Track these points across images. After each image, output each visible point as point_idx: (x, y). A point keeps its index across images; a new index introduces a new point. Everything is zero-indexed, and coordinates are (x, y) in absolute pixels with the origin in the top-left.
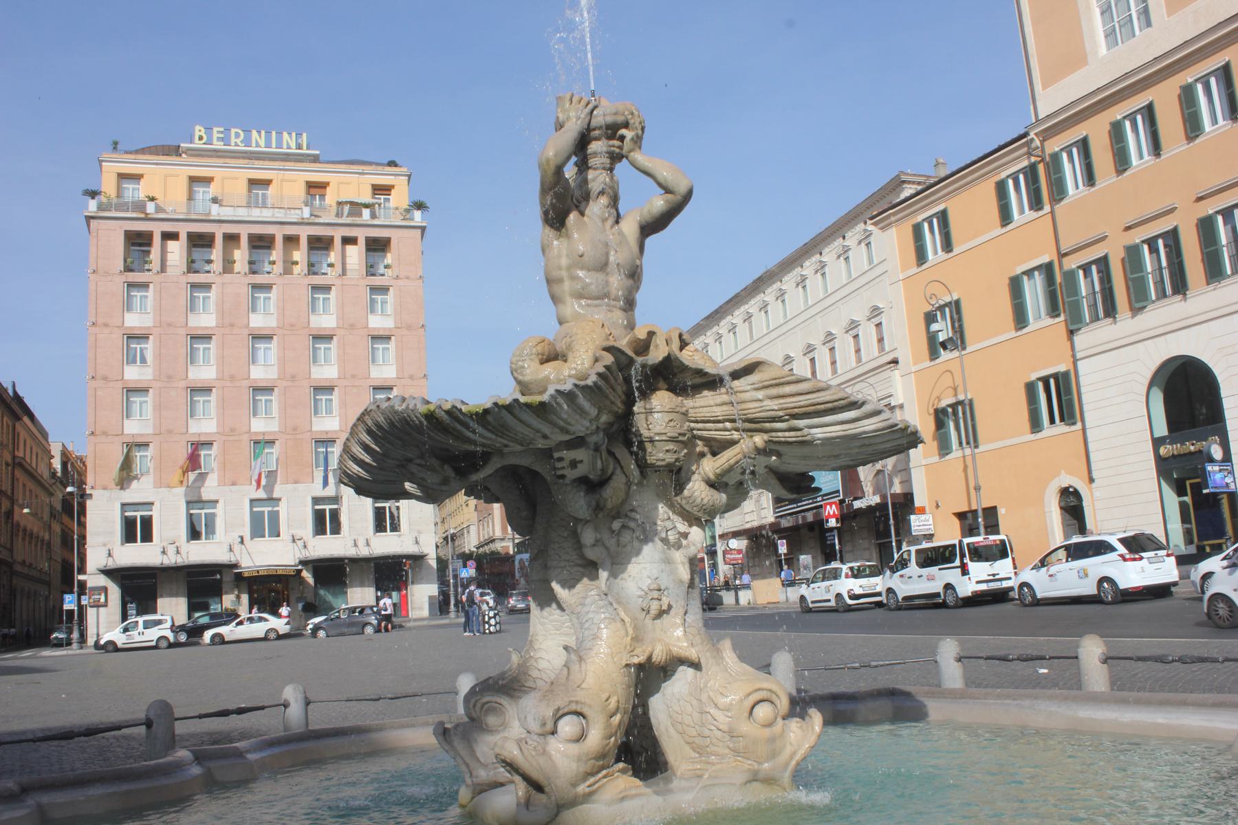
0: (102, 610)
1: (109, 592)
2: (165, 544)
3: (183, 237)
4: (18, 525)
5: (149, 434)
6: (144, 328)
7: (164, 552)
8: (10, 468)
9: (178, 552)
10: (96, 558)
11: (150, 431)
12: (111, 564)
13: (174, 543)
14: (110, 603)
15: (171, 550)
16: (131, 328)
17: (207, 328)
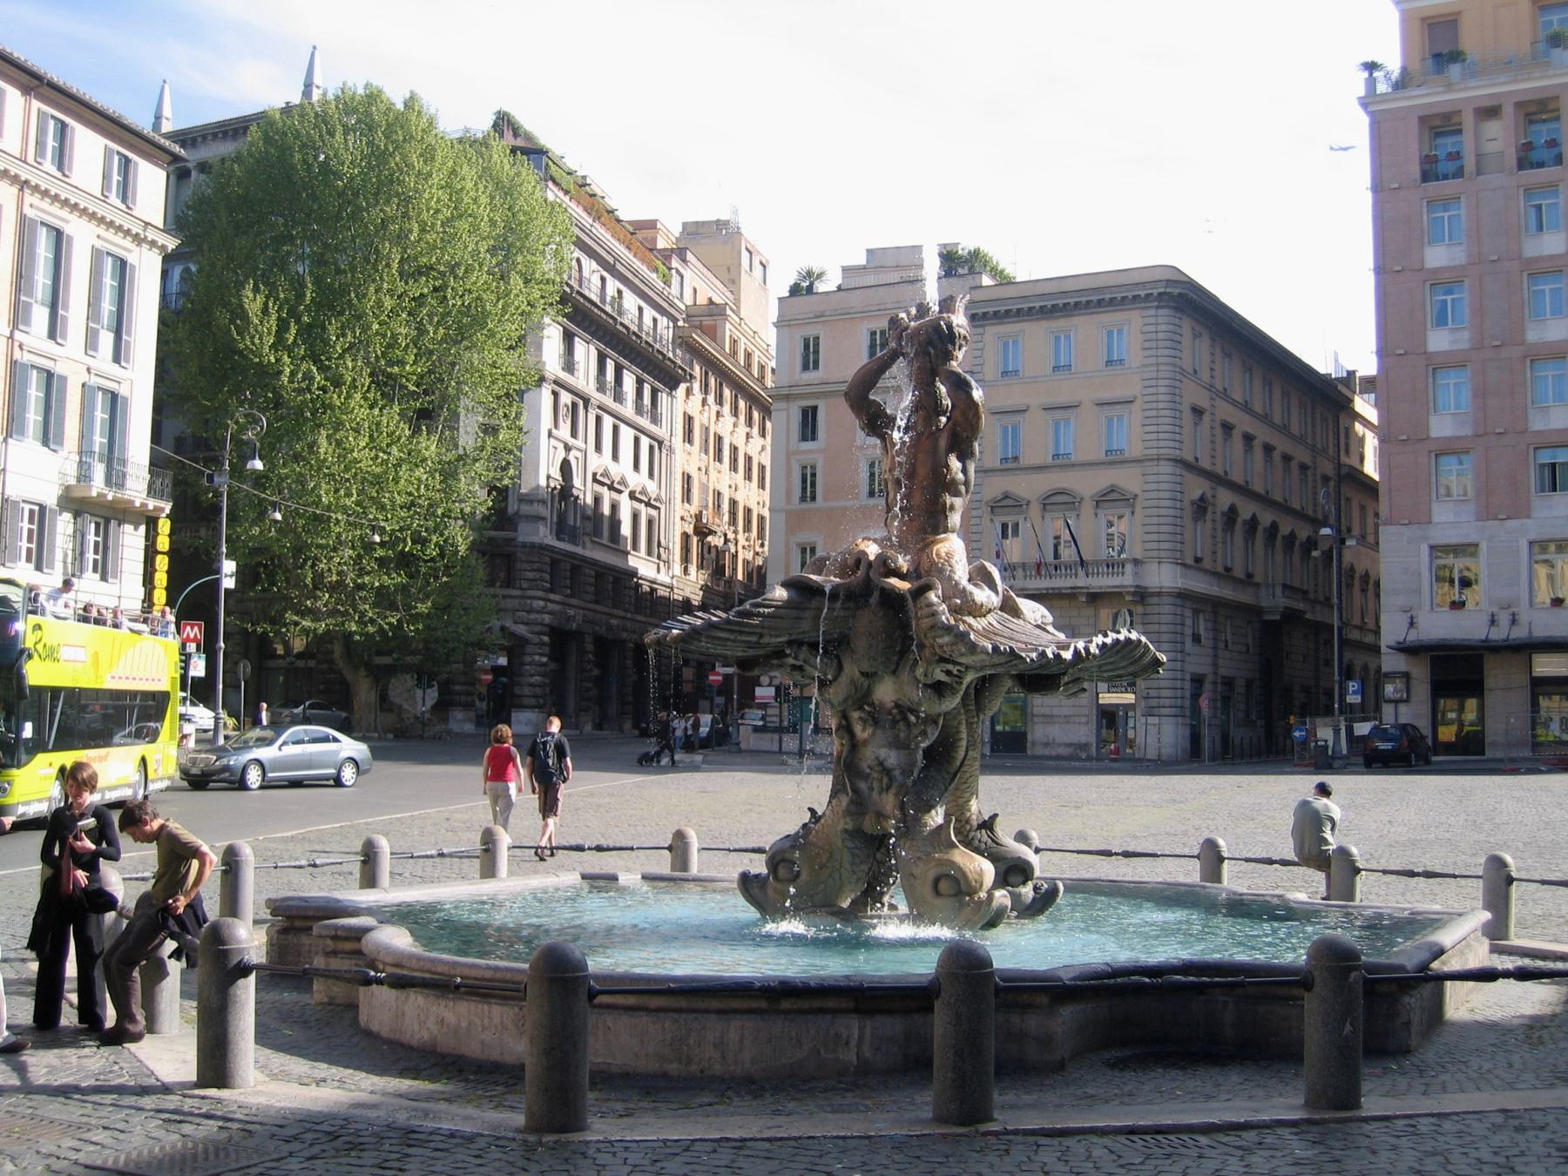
0: (1403, 708)
1: (1413, 682)
2: (1495, 610)
3: (1508, 110)
4: (1352, 569)
5: (1467, 437)
6: (1455, 268)
7: (1493, 622)
8: (1332, 484)
9: (1514, 621)
10: (1392, 630)
11: (1467, 431)
12: (1413, 637)
13: (1509, 607)
14: (1413, 698)
15: (1504, 618)
16: (1436, 270)
17: (1552, 257)
